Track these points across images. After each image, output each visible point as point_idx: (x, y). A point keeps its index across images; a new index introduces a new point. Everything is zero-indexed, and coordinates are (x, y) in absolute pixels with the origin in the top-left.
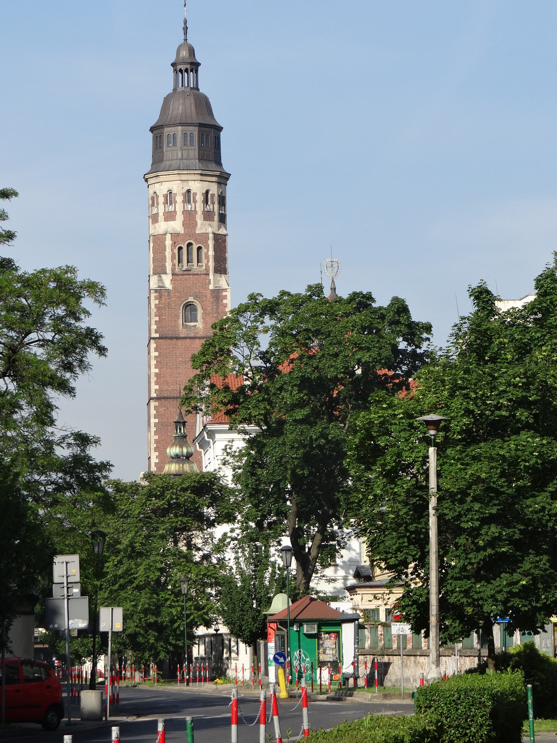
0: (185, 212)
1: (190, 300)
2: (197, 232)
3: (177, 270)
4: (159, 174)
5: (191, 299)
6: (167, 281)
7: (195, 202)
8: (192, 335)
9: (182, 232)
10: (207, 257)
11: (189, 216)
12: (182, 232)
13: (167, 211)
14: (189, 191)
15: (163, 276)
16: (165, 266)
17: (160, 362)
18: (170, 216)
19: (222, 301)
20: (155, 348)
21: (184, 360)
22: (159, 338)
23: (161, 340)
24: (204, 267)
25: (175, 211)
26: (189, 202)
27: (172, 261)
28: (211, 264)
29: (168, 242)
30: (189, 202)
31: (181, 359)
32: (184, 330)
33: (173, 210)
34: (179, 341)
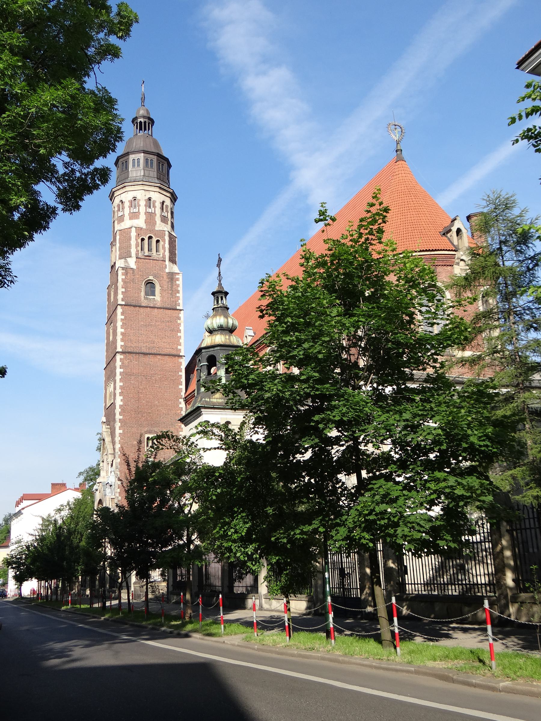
0: (146, 213)
1: (150, 278)
2: (156, 229)
3: (140, 255)
4: (126, 184)
5: (151, 278)
6: (132, 262)
7: (154, 207)
8: (152, 305)
9: (144, 227)
10: (164, 248)
11: (150, 217)
12: (144, 227)
13: (132, 212)
14: (150, 199)
15: (128, 259)
16: (130, 252)
17: (126, 324)
18: (134, 216)
19: (175, 281)
20: (122, 313)
22: (125, 305)
23: (126, 307)
24: (161, 256)
25: (139, 212)
26: (150, 207)
27: (136, 248)
28: (167, 254)
29: (133, 234)
30: (150, 207)
32: (146, 301)
33: (137, 211)
34: (141, 308)
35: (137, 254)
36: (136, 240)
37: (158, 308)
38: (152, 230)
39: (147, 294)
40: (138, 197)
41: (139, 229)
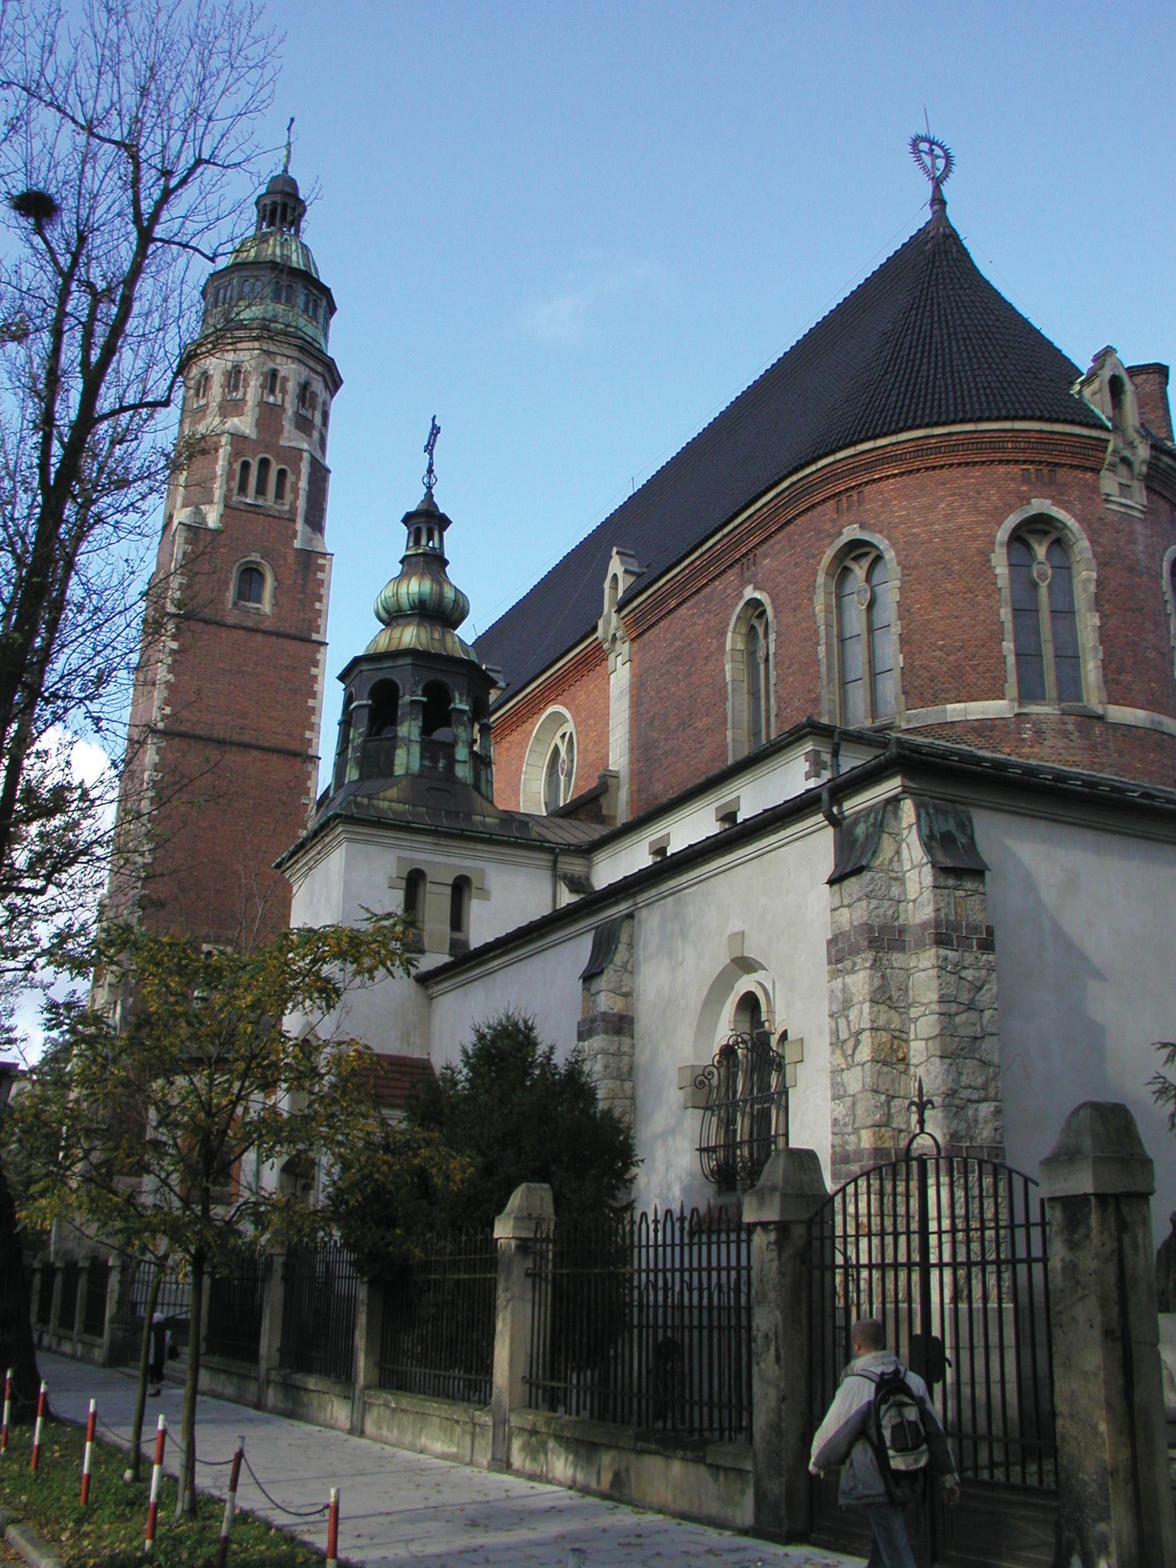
1: (252, 559)
5: (255, 557)
8: (250, 624)
9: (254, 436)
12: (254, 436)
18: (230, 407)
21: (228, 668)
27: (228, 482)
31: (222, 665)
34: (224, 629)
35: (227, 498)
36: (230, 464)
37: (264, 632)
38: (272, 446)
39: (242, 595)
40: (246, 366)
41: (237, 439)
